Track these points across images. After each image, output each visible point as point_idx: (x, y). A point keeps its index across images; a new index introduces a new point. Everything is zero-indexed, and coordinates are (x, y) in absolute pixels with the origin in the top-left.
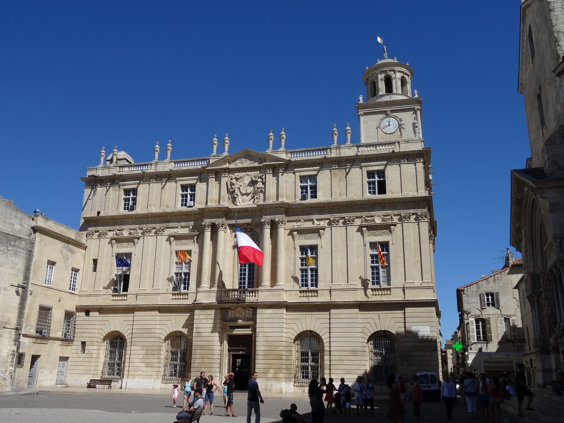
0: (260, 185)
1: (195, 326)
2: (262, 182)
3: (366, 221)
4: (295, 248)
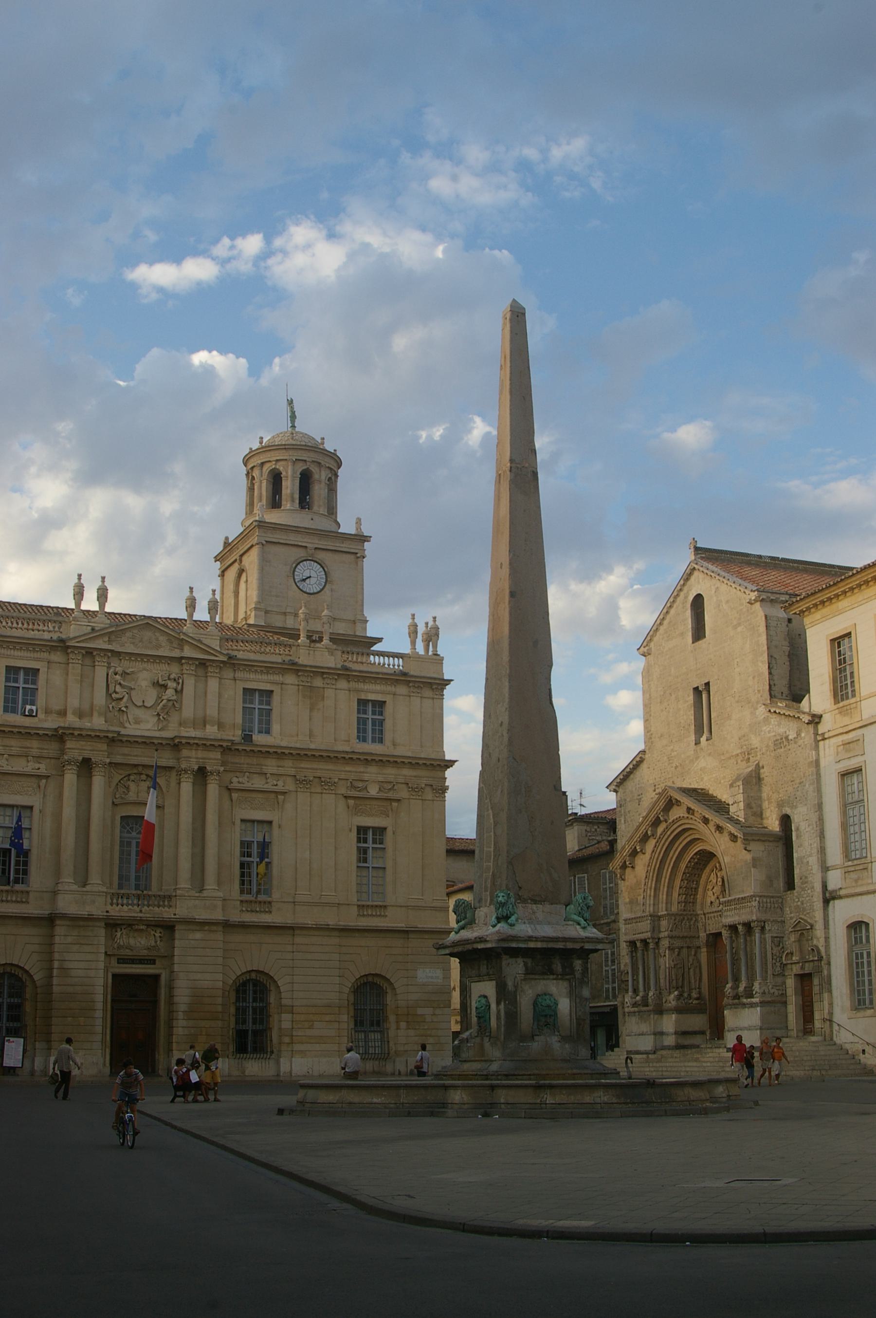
0: (170, 693)
1: (56, 956)
2: (176, 691)
3: (353, 787)
4: (234, 823)
